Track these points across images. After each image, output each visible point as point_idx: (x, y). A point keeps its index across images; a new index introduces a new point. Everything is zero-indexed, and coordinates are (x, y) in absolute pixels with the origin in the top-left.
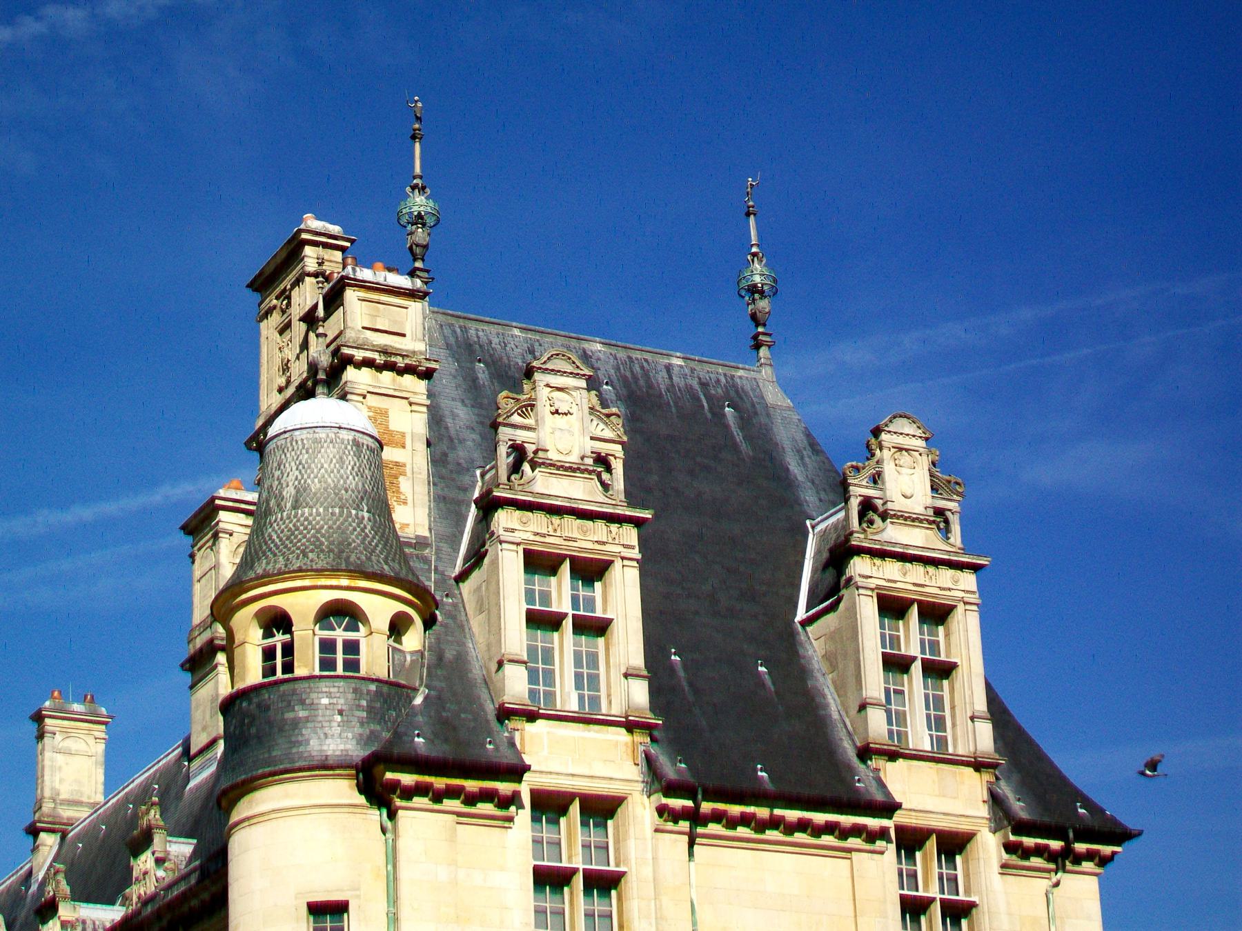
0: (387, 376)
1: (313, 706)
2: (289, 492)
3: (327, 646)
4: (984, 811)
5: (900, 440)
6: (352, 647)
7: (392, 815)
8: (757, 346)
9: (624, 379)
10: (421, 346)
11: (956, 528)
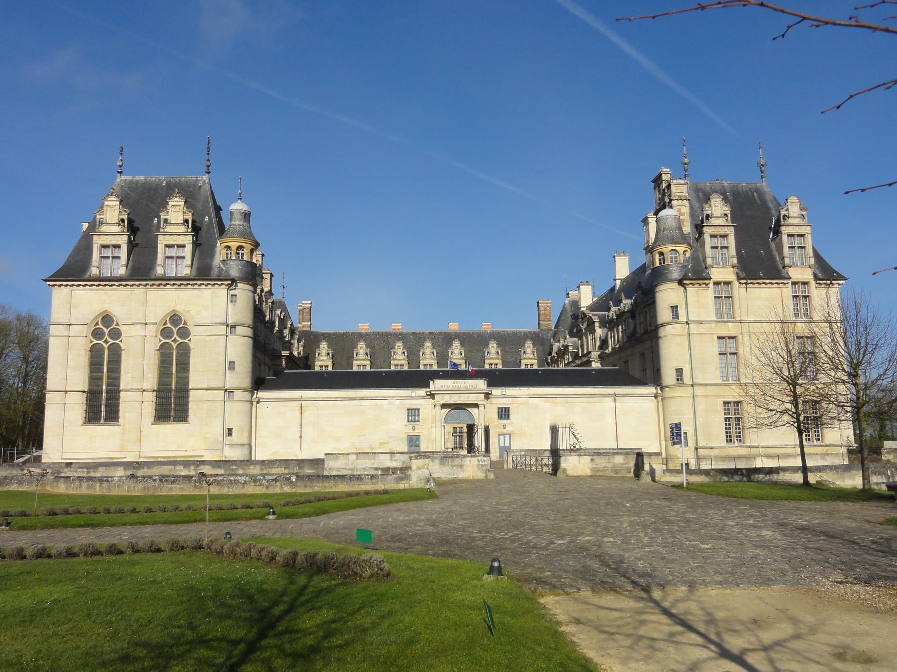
0: (680, 201)
1: (669, 270)
2: (662, 228)
3: (671, 258)
4: (812, 277)
5: (792, 201)
6: (676, 258)
7: (685, 289)
8: (762, 178)
9: (732, 191)
10: (687, 194)
11: (806, 218)
